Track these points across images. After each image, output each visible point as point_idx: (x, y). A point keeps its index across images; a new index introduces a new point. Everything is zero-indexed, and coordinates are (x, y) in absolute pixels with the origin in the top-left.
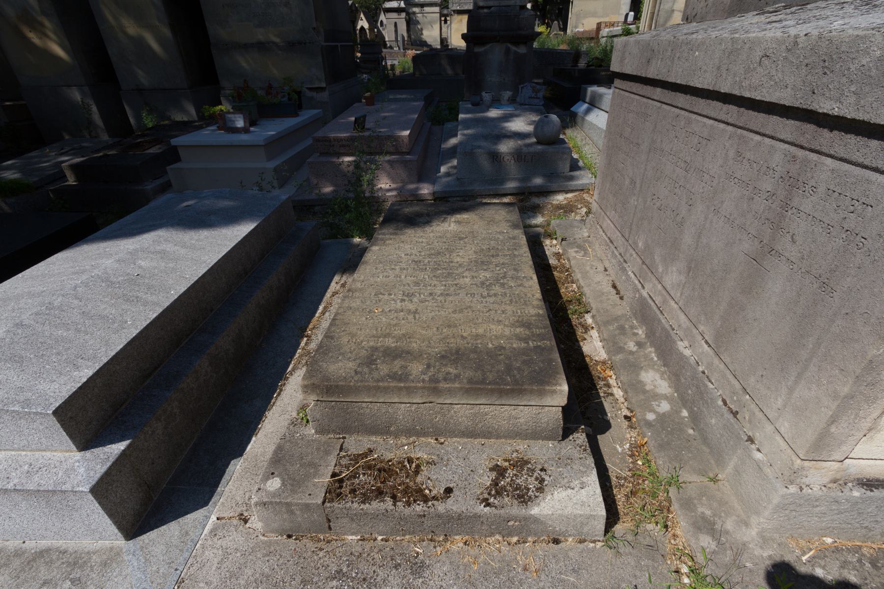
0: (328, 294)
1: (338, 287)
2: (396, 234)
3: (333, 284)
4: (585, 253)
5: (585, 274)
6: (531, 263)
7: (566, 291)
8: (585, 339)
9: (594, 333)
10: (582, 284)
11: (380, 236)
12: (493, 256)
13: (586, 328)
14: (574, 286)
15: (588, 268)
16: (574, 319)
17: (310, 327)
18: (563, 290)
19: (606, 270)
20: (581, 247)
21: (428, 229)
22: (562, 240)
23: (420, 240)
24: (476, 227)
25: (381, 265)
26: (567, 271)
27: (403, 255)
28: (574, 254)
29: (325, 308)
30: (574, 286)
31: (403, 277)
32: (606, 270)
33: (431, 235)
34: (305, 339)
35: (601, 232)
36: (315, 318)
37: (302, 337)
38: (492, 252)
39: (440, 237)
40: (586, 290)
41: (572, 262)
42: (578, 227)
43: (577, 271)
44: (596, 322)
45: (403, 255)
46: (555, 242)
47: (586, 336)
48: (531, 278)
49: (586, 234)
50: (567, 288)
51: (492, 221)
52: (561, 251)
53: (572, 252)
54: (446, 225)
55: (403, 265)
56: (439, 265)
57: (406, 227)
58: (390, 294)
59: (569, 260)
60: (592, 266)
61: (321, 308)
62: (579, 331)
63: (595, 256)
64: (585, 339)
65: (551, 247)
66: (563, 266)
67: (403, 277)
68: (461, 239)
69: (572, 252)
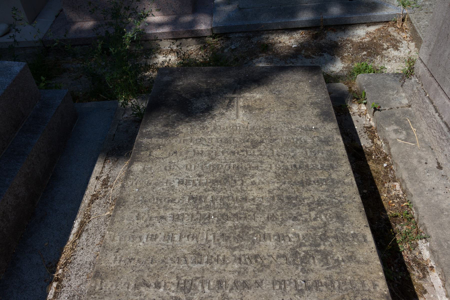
0: (86, 200)
1: (99, 186)
2: (165, 135)
3: (93, 180)
4: (408, 134)
5: (412, 170)
6: (358, 199)
7: (390, 193)
8: (425, 292)
9: (435, 278)
10: (411, 190)
11: (145, 141)
12: (302, 184)
13: (424, 269)
14: (397, 185)
15: (415, 162)
16: (407, 256)
17: (62, 261)
18: (384, 196)
19: (440, 167)
20: (402, 125)
21: (209, 123)
22: (375, 109)
23: (200, 148)
24: (273, 118)
25: (145, 209)
26: (385, 159)
27: (176, 184)
28: (393, 136)
29: (82, 224)
30: (397, 185)
31: (177, 237)
32: (440, 167)
33: (214, 135)
34: (55, 284)
35: (433, 111)
36: (69, 245)
37: (51, 283)
38: (301, 175)
39: (227, 141)
40: (416, 200)
41: (393, 150)
42: (393, 89)
43: (401, 165)
44: (438, 262)
45: (176, 184)
46: (363, 107)
47: (426, 286)
48: (364, 237)
49: (405, 102)
50: (389, 192)
51: (293, 107)
52: (373, 123)
53: (390, 130)
54: (231, 114)
55: (177, 208)
56: (228, 207)
57: (180, 120)
58: (158, 286)
59: (387, 143)
60: (420, 158)
61: (76, 224)
62: (415, 274)
63: (422, 140)
64: (425, 292)
65: (361, 115)
66: (378, 148)
67: (177, 237)
68: (255, 144)
69: (390, 130)
